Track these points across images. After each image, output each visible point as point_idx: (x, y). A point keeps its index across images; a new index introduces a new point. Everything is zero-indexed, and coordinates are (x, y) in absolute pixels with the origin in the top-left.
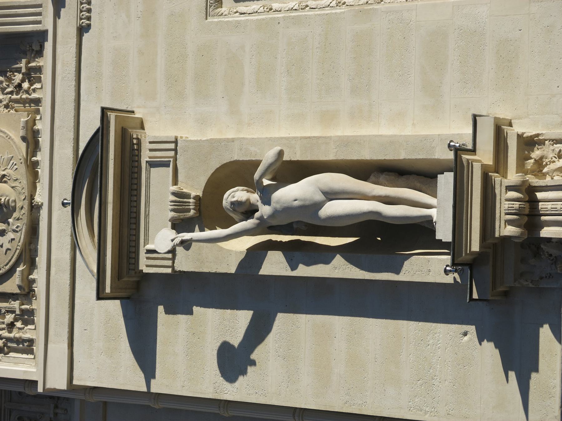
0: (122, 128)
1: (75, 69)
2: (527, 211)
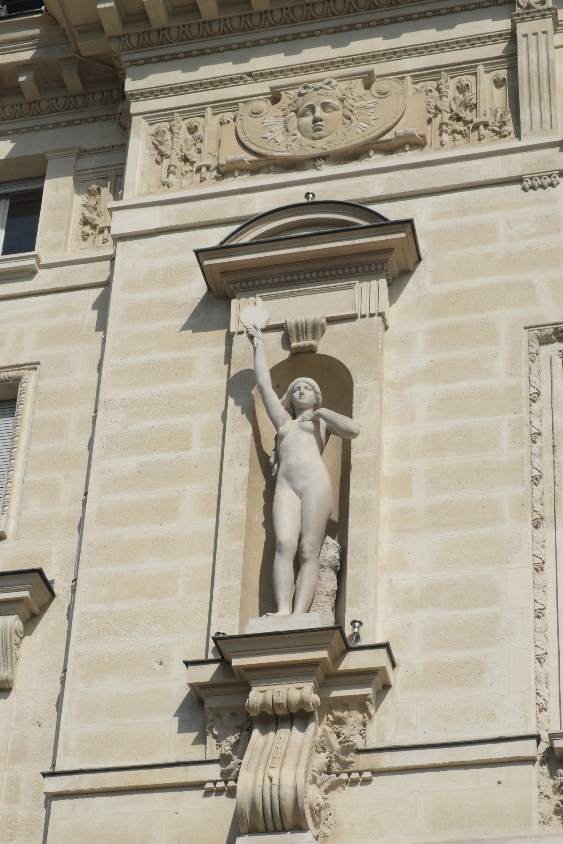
0: (393, 248)
1: (472, 181)
2: (279, 712)
